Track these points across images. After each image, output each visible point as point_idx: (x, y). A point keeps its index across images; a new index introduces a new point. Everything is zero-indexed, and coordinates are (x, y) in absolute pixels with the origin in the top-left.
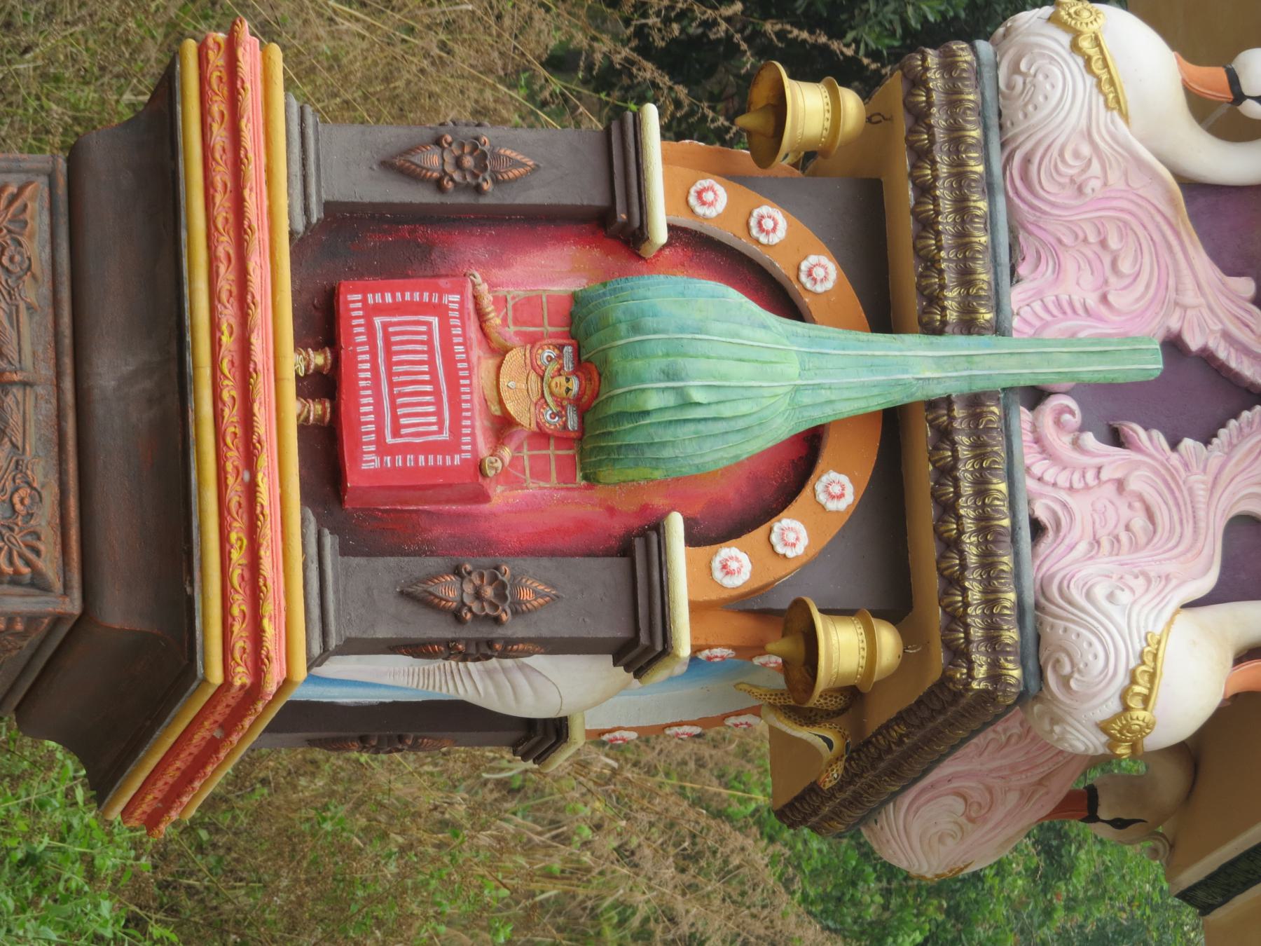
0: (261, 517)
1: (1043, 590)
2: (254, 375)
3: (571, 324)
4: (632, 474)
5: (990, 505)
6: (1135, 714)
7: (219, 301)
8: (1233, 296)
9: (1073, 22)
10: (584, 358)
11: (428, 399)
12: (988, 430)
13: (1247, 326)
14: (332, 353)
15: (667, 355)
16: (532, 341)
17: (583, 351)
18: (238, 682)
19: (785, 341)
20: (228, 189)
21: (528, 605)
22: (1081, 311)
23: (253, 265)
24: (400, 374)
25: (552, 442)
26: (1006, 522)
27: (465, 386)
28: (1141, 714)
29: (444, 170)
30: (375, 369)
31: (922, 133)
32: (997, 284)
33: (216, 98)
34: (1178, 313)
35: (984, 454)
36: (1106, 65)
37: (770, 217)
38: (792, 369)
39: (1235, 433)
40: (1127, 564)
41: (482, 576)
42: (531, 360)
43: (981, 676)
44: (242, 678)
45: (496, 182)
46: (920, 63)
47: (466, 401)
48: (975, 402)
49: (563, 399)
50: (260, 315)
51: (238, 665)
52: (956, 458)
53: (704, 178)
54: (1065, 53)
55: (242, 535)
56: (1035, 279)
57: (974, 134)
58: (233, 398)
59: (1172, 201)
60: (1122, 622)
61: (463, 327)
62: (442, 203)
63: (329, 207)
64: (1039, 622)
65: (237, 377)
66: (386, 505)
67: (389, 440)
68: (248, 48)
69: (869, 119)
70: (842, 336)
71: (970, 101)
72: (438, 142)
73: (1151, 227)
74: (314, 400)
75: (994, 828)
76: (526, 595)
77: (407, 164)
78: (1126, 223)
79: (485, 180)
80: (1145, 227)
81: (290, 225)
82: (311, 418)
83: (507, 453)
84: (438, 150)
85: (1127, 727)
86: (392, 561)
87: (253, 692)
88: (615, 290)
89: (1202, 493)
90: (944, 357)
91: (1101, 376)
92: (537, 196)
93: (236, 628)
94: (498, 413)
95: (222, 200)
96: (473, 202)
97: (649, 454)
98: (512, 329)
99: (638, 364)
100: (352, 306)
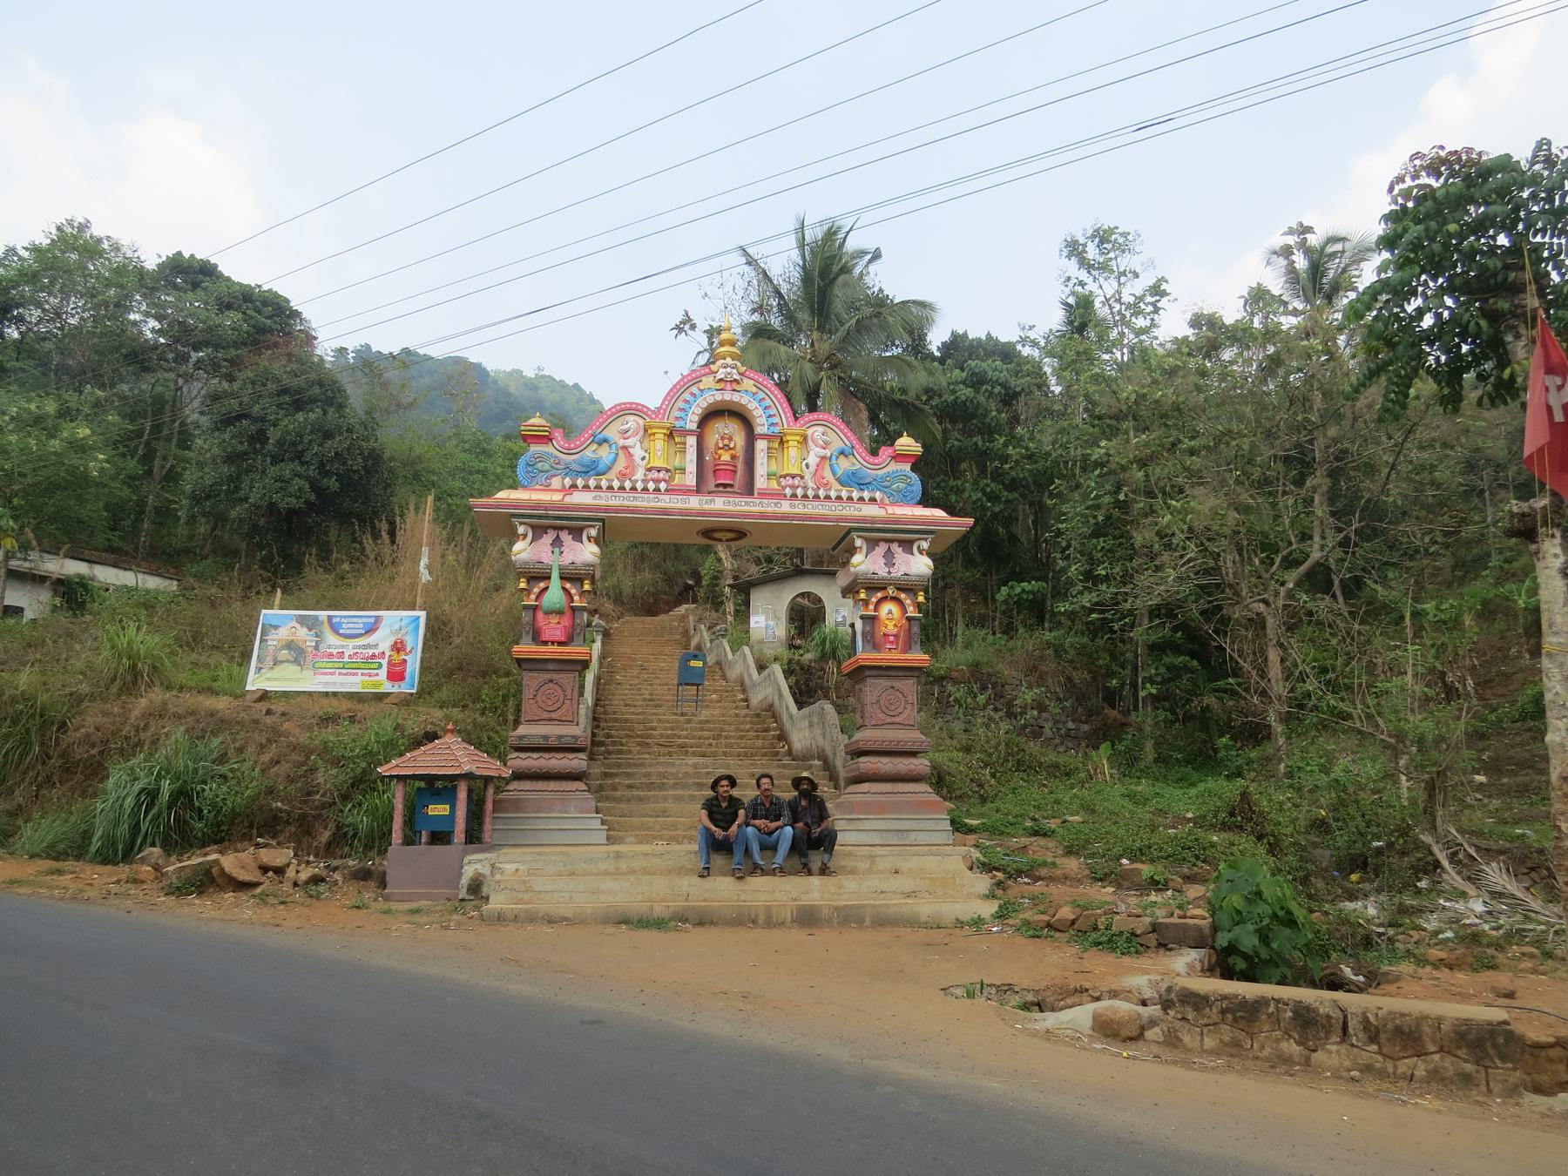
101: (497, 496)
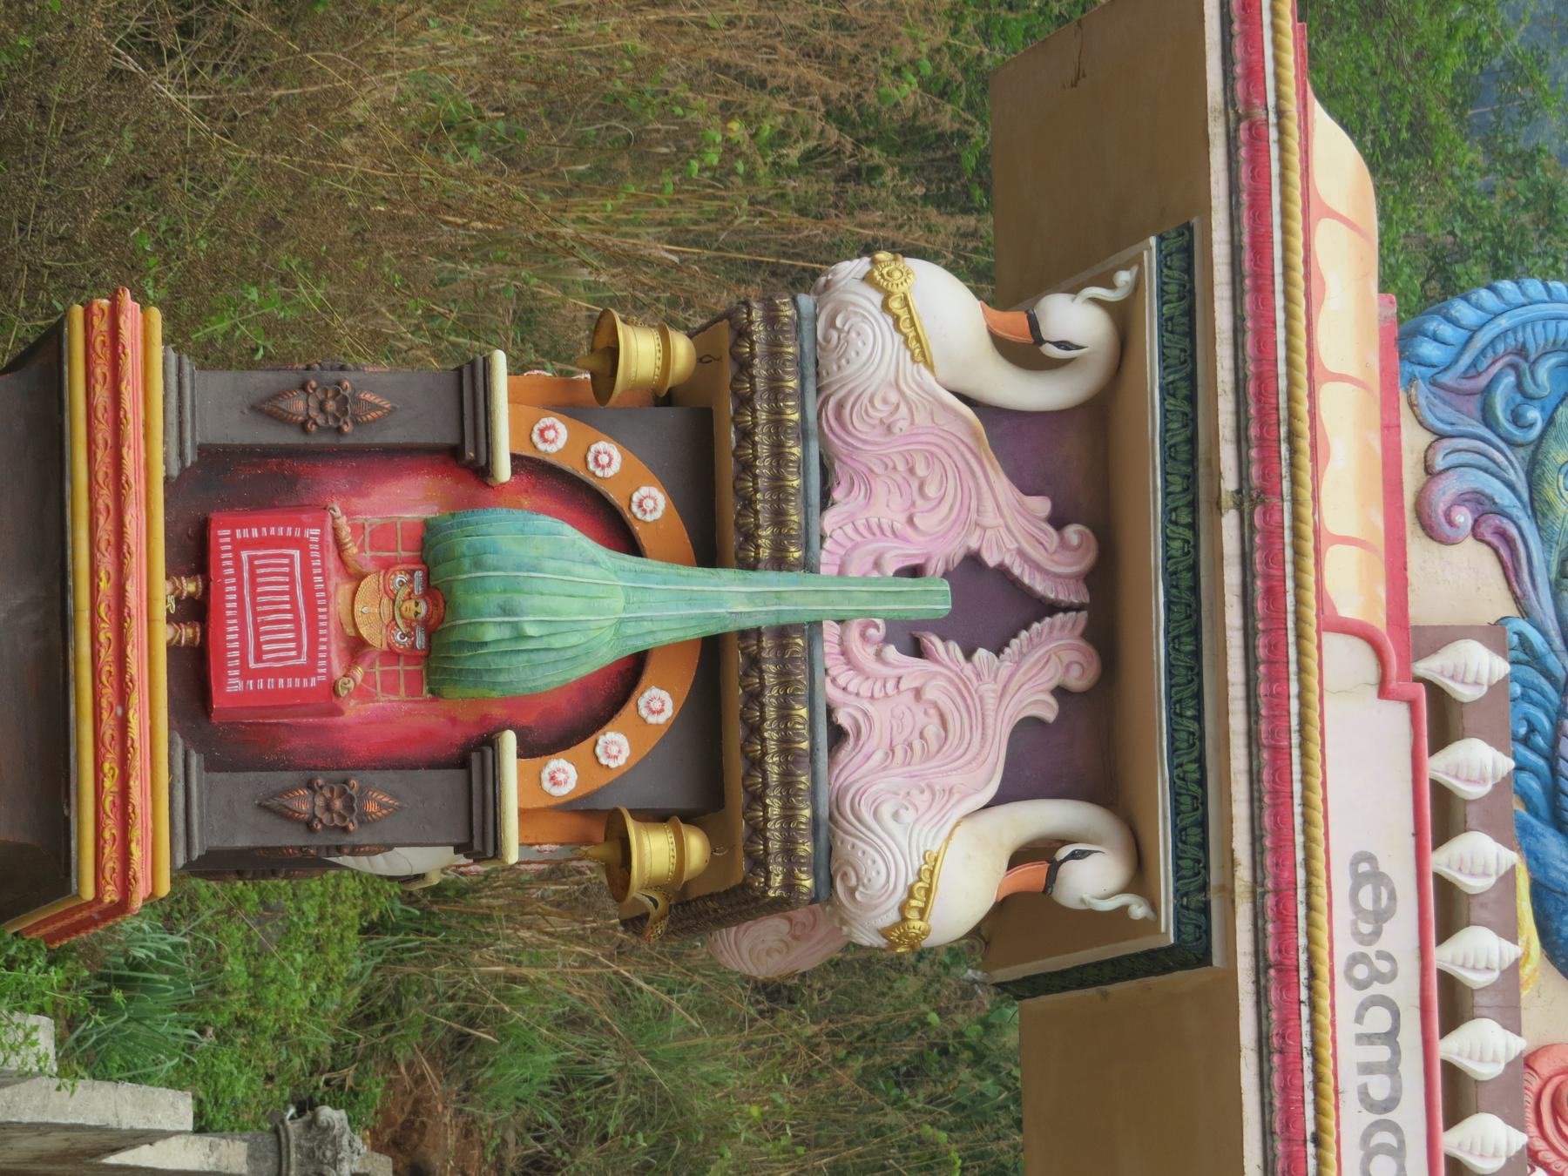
1: (836, 804)
3: (422, 549)
4: (471, 693)
5: (792, 729)
10: (432, 583)
11: (288, 626)
12: (793, 660)
13: (1041, 544)
14: (203, 580)
15: (505, 591)
17: (432, 577)
18: (107, 899)
19: (612, 576)
23: (130, 518)
24: (263, 604)
25: (402, 658)
26: (805, 745)
27: (322, 613)
28: (918, 924)
30: (240, 600)
31: (743, 381)
32: (807, 524)
33: (99, 361)
34: (978, 532)
36: (913, 324)
39: (1025, 643)
41: (332, 791)
44: (111, 895)
45: (355, 423)
47: (324, 628)
48: (782, 633)
50: (135, 564)
52: (762, 685)
53: (547, 416)
54: (876, 312)
55: (114, 765)
57: (791, 384)
59: (974, 433)
60: (904, 842)
61: (322, 559)
63: (204, 450)
64: (831, 835)
67: (252, 665)
69: (700, 360)
70: (665, 570)
72: (303, 387)
73: (956, 456)
75: (818, 943)
76: (371, 807)
78: (932, 454)
79: (345, 423)
80: (950, 456)
81: (166, 471)
83: (359, 672)
84: (303, 396)
85: (905, 935)
86: (252, 775)
87: (122, 907)
89: (991, 701)
92: (394, 435)
93: (107, 851)
94: (353, 634)
95: (102, 456)
97: (486, 679)
98: (369, 554)
99: (478, 598)
100: (221, 540)
101: (1322, 120)
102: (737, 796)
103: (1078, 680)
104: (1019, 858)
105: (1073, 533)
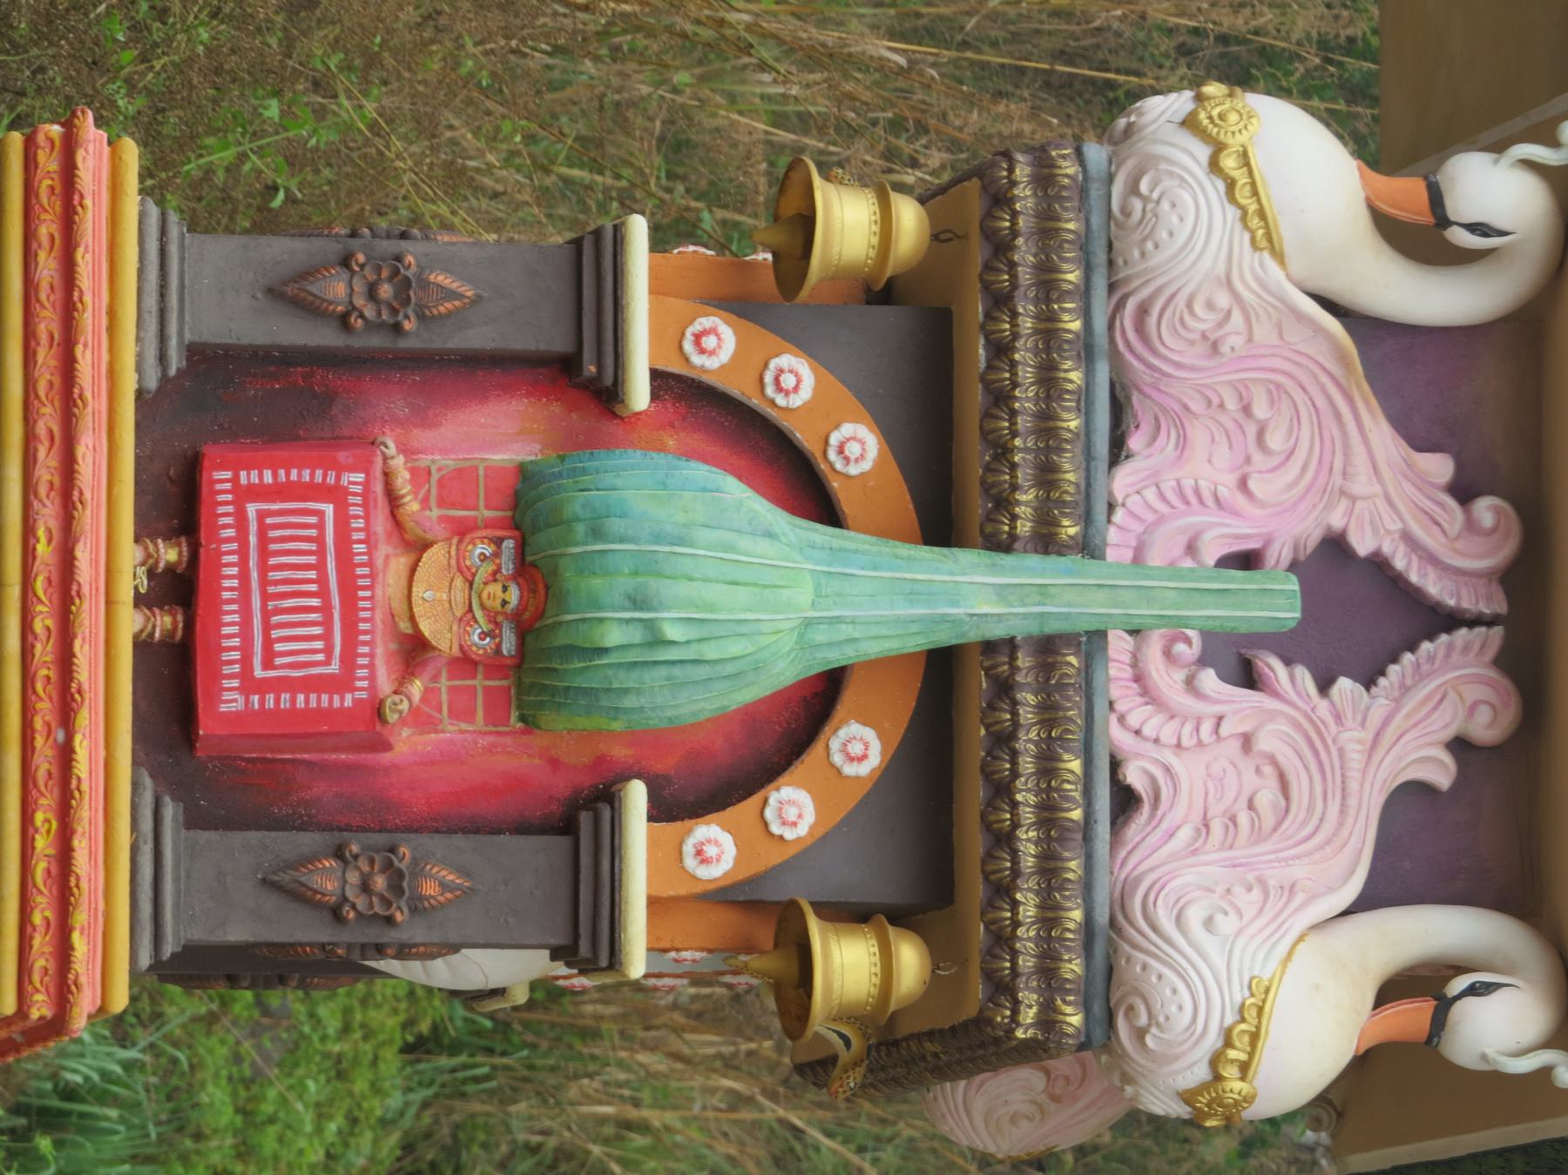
0: (77, 794)
1: (1121, 903)
2: (77, 601)
3: (515, 507)
4: (583, 722)
5: (1058, 790)
6: (1229, 1085)
7: (36, 496)
8: (1420, 480)
9: (1215, 130)
10: (529, 559)
12: (1061, 687)
13: (1438, 524)
14: (189, 544)
15: (636, 573)
16: (462, 530)
17: (528, 550)
18: (35, 1014)
19: (799, 558)
20: (55, 343)
21: (432, 901)
22: (1210, 502)
23: (83, 451)
24: (276, 583)
25: (480, 669)
26: (1076, 814)
27: (364, 599)
28: (1238, 1085)
29: (351, 303)
30: (244, 576)
31: (1000, 271)
32: (1088, 485)
33: (44, 216)
34: (1344, 504)
35: (1054, 720)
36: (1255, 193)
37: (791, 371)
38: (802, 596)
39: (1409, 671)
40: (1240, 865)
41: (372, 862)
42: (458, 559)
43: (1029, 1021)
44: (41, 1008)
45: (422, 317)
46: (1005, 173)
47: (365, 620)
48: (1048, 647)
49: (497, 613)
50: (89, 519)
51: (38, 991)
52: (1016, 724)
53: (706, 315)
54: (1201, 173)
55: (50, 815)
56: (1150, 456)
57: (1071, 277)
58: (48, 629)
59: (1343, 359)
60: (1219, 961)
61: (367, 518)
62: (347, 346)
63: (197, 353)
65: (55, 601)
66: (251, 752)
67: (259, 673)
68: (91, 149)
69: (935, 237)
70: (875, 549)
71: (1069, 231)
72: (346, 262)
73: (1314, 390)
74: (161, 608)
75: (1088, 1107)
76: (429, 889)
77: (303, 295)
78: (1279, 386)
79: (407, 317)
80: (1304, 390)
81: (139, 382)
82: (157, 635)
83: (416, 688)
84: (345, 275)
85: (1218, 1101)
86: (253, 836)
87: (56, 1025)
88: (574, 469)
89: (1356, 756)
90: (1009, 585)
91: (1217, 623)
92: (479, 338)
93: (37, 942)
94: (409, 631)
95: (46, 357)
96: (388, 345)
97: (605, 702)
98: (435, 512)
99: (596, 582)
100: (219, 487)
102: (973, 889)
103: (1486, 728)
104: (1391, 991)
105: (1486, 509)
